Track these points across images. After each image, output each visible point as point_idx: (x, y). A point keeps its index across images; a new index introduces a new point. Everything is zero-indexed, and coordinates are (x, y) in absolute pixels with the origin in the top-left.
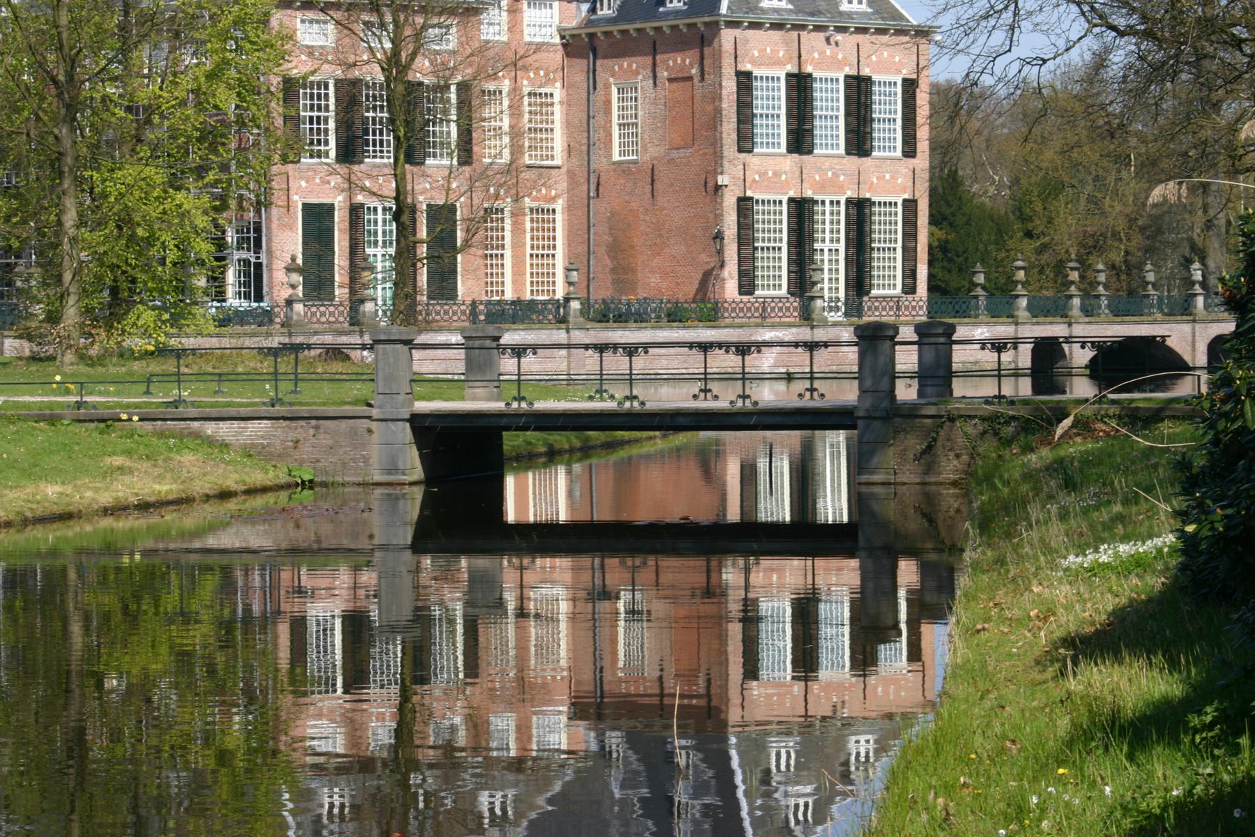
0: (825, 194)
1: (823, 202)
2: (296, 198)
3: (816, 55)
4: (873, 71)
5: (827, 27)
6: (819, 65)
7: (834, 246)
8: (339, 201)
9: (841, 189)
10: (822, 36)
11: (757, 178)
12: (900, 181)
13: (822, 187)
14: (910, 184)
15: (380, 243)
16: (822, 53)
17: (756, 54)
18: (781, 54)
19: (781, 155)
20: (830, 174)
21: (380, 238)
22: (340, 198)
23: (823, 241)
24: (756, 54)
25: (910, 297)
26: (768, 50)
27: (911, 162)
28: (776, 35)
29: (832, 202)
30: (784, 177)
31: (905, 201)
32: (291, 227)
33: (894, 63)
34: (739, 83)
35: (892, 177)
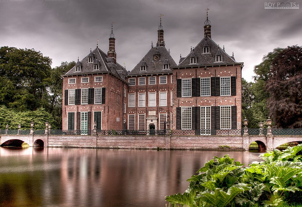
0: (204, 106)
2: (67, 112)
3: (202, 74)
4: (221, 76)
5: (205, 67)
6: (202, 76)
7: (208, 118)
8: (76, 112)
9: (210, 104)
10: (203, 69)
11: (183, 103)
13: (203, 104)
15: (84, 120)
17: (183, 75)
18: (191, 74)
19: (190, 97)
20: (206, 101)
21: (84, 119)
22: (76, 111)
23: (204, 117)
24: (183, 75)
26: (187, 74)
28: (189, 70)
29: (207, 108)
30: (191, 102)
32: (66, 117)
33: (228, 73)
34: (177, 82)
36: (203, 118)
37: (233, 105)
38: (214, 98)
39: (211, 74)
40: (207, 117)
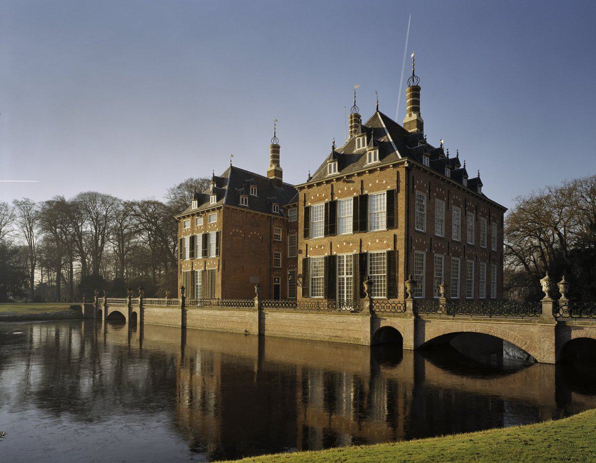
1: (344, 256)
3: (340, 191)
12: (385, 242)
13: (341, 250)
14: (392, 243)
16: (342, 190)
17: (313, 198)
20: (345, 244)
25: (391, 301)
27: (395, 231)
29: (347, 256)
30: (323, 247)
31: (389, 253)
33: (383, 184)
35: (381, 241)
36: (349, 276)
37: (390, 249)
38: (359, 236)
39: (354, 191)
40: (347, 274)
